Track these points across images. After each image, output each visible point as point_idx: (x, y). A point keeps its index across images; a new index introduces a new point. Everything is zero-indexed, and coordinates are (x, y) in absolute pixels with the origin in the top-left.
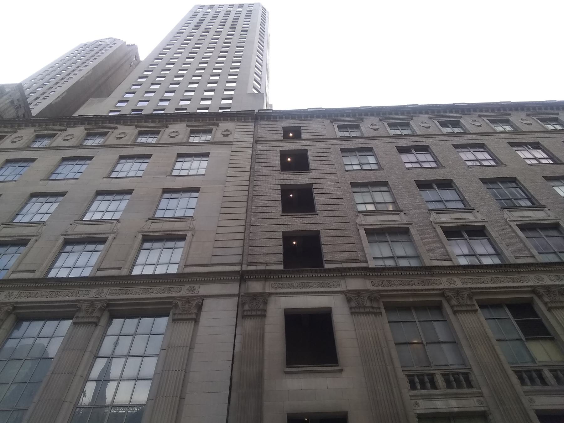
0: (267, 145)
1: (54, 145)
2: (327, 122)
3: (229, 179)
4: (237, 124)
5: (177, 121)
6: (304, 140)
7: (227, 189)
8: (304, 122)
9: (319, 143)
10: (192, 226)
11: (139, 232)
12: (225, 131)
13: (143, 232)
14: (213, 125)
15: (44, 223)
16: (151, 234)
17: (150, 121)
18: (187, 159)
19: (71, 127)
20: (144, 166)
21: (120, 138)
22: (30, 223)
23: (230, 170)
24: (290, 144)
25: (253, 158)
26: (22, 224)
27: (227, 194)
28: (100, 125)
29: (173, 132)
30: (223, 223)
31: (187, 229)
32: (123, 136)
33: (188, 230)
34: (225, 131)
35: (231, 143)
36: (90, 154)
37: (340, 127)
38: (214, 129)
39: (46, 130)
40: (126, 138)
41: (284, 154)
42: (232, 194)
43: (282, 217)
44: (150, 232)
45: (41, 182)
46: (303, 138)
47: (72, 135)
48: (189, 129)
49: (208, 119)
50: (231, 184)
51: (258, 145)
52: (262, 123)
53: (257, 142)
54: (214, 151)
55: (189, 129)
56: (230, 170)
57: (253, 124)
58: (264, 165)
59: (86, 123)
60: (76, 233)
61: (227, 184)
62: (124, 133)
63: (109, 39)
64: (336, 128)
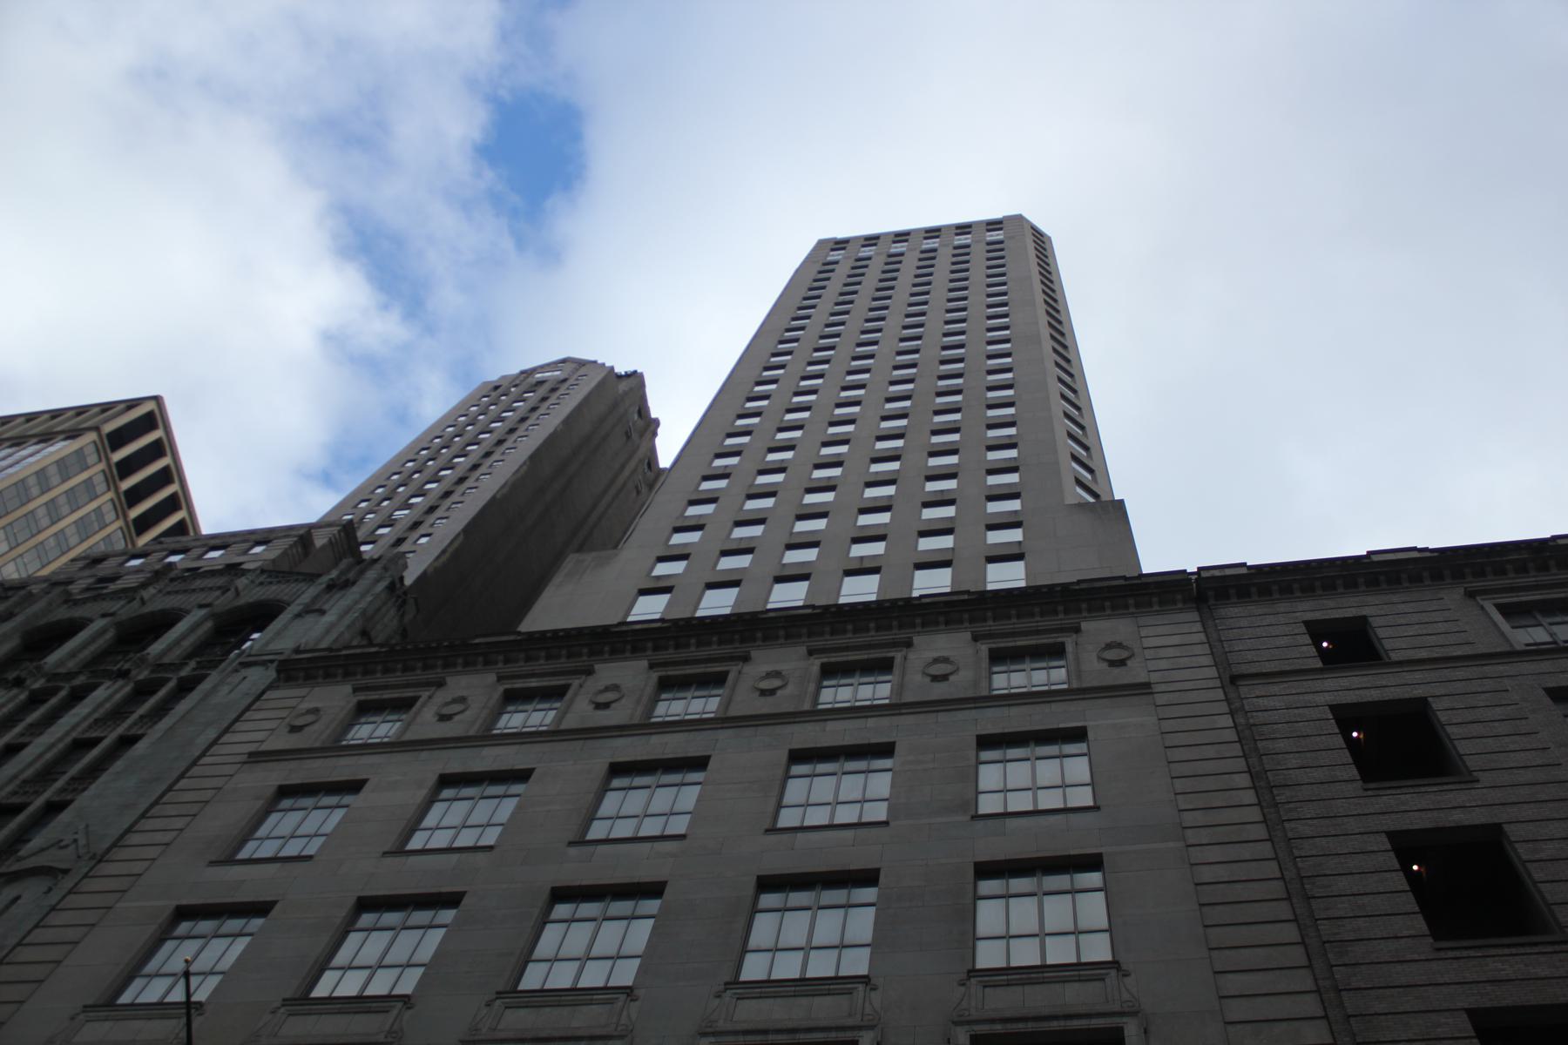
0: (1275, 689)
1: (570, 722)
2: (1452, 596)
3: (1189, 819)
4: (1143, 620)
5: (937, 623)
6: (1400, 663)
7: (1197, 855)
8: (1371, 599)
9: (1460, 674)
10: (1126, 996)
11: (956, 1023)
12: (1109, 646)
13: (969, 1023)
14: (1062, 630)
15: (628, 991)
16: (998, 1028)
17: (850, 627)
18: (1013, 753)
19: (605, 661)
20: (881, 784)
21: (772, 692)
22: (576, 996)
23: (1180, 785)
24: (1356, 681)
25: (1248, 737)
26: (546, 997)
27: (1207, 874)
28: (693, 652)
29: (936, 661)
30: (1233, 984)
31: (1116, 1008)
32: (776, 683)
33: (1122, 1014)
34: (1109, 646)
35: (1144, 688)
36: (694, 751)
37: (1507, 611)
38: (1069, 642)
39: (533, 675)
40: (790, 690)
41: (1345, 716)
42: (1222, 873)
43: (1442, 954)
44: (993, 1021)
45: (573, 851)
46: (1395, 656)
47: (615, 688)
48: (984, 648)
49: (1037, 610)
50: (1204, 836)
51: (1244, 691)
52: (1223, 612)
53: (1234, 679)
54: (1098, 718)
55: (984, 648)
56: (1180, 785)
57: (1195, 616)
58: (1293, 761)
59: (650, 645)
60: (745, 1026)
61: (1192, 836)
62: (777, 674)
63: (564, 361)
64: (1497, 617)
